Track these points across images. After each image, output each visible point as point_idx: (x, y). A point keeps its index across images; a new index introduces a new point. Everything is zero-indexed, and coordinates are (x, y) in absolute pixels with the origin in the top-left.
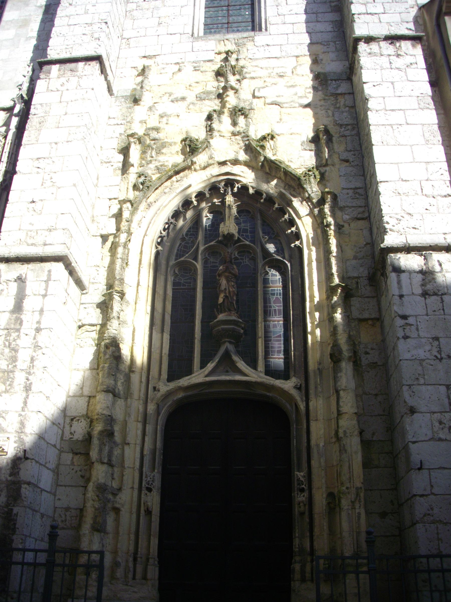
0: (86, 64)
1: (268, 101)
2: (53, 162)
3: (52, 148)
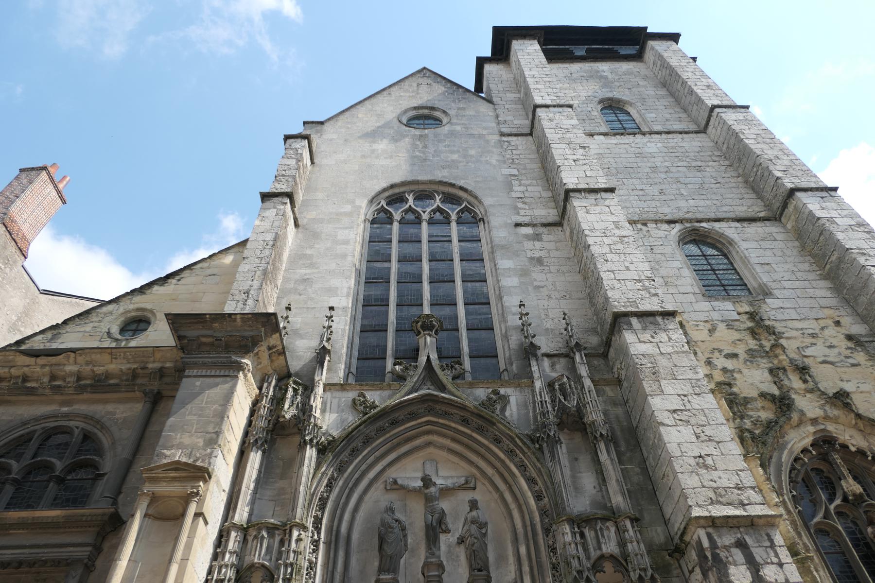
0: (664, 319)
1: (820, 360)
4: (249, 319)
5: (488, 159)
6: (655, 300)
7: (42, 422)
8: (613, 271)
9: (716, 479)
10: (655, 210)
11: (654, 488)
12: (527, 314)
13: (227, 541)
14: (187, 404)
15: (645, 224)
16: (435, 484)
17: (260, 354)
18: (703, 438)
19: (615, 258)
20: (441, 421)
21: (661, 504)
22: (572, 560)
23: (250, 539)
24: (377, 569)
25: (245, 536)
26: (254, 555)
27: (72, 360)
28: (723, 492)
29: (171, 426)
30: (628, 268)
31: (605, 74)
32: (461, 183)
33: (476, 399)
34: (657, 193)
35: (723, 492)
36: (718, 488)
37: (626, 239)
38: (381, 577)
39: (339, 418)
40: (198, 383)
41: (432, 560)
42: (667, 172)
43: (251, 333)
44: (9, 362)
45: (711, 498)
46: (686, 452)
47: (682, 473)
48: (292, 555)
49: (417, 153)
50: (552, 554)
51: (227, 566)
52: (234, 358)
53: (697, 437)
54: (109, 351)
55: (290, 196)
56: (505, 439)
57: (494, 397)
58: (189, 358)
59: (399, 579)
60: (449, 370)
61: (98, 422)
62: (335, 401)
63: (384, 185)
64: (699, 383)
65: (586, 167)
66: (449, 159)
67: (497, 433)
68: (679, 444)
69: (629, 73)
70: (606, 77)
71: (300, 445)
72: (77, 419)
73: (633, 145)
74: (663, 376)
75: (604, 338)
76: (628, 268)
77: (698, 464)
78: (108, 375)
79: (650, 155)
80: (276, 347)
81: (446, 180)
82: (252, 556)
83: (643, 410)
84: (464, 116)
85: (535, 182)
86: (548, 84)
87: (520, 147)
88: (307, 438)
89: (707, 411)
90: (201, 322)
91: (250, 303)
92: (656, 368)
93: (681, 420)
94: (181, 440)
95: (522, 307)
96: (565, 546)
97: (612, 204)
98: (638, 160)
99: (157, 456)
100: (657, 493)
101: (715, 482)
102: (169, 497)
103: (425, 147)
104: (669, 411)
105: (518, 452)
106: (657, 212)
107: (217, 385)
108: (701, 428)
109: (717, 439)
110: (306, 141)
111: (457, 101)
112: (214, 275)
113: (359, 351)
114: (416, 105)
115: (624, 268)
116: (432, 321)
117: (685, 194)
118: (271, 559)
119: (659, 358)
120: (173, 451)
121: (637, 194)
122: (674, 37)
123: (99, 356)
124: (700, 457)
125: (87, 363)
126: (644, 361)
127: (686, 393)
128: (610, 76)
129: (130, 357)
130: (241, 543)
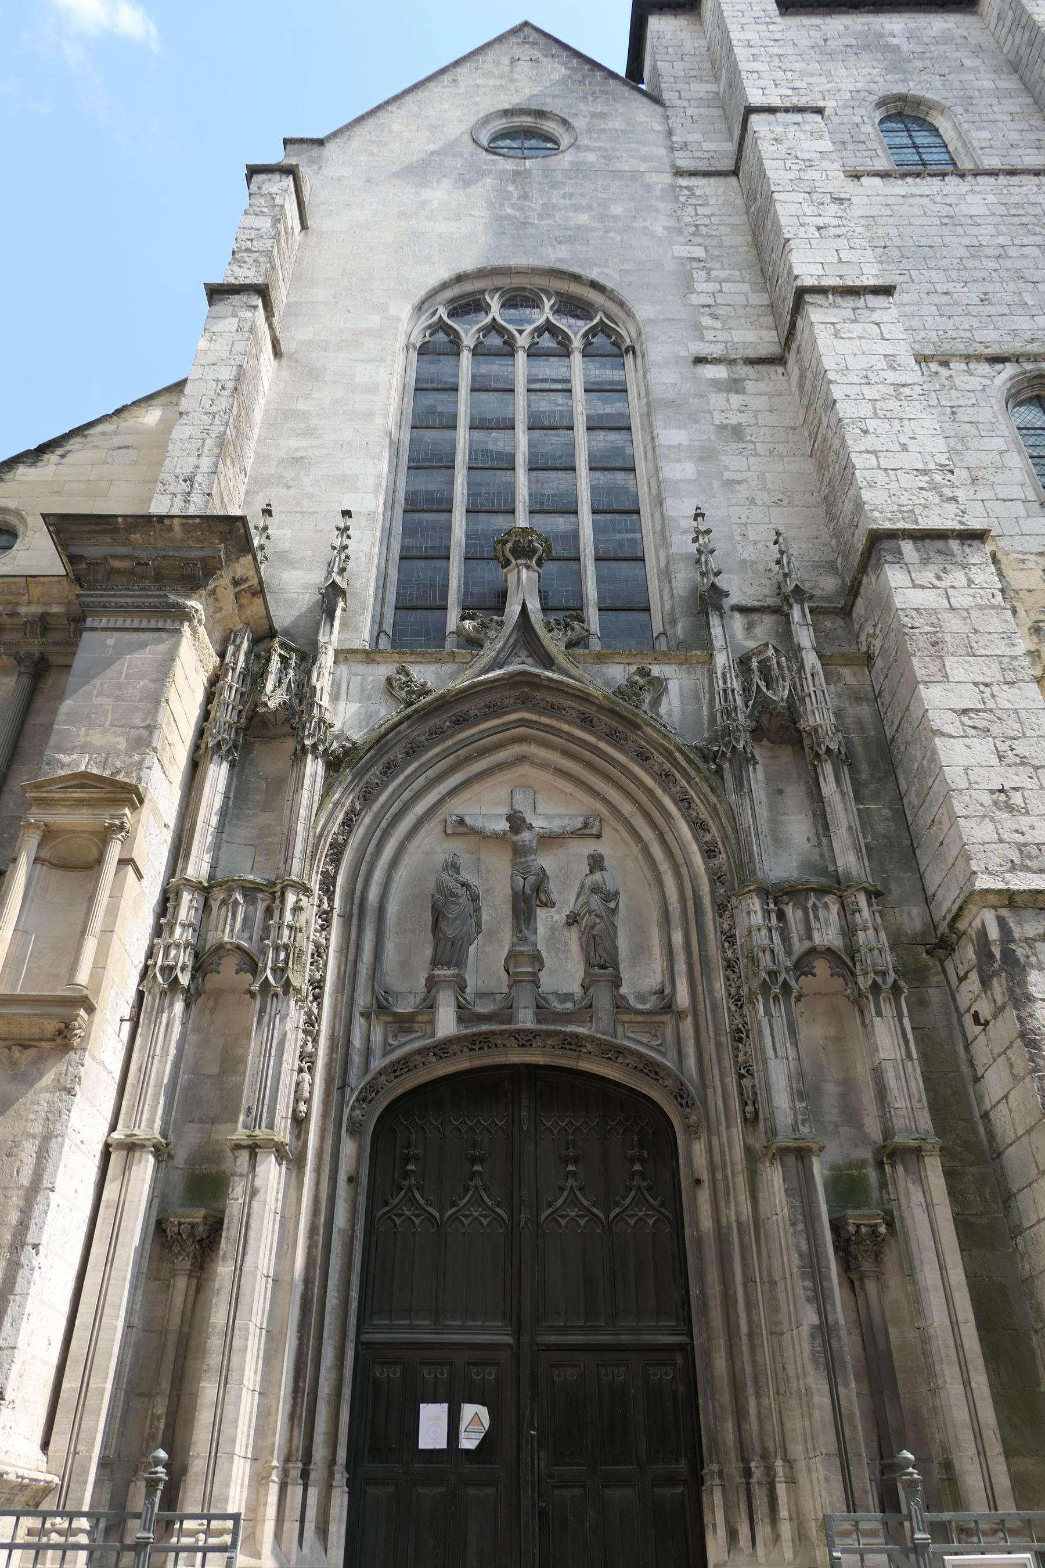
0: (963, 544)
2: (999, 719)
3: (983, 692)
4: (197, 527)
5: (648, 224)
6: (951, 508)
8: (875, 453)
9: (1024, 829)
10: (969, 334)
11: (912, 844)
12: (708, 532)
13: (177, 907)
14: (93, 677)
15: (945, 364)
16: (530, 827)
17: (218, 592)
18: (1011, 758)
19: (882, 426)
20: (544, 720)
21: (922, 870)
22: (761, 955)
23: (215, 905)
24: (429, 960)
25: (206, 900)
26: (223, 931)
28: (1035, 851)
29: (67, 714)
30: (904, 448)
31: (895, 41)
32: (594, 274)
33: (607, 684)
34: (977, 301)
35: (1035, 851)
36: (1026, 845)
37: (906, 391)
38: (437, 972)
39: (363, 710)
40: (111, 640)
41: (522, 949)
42: (999, 256)
43: (201, 554)
45: (1012, 861)
46: (976, 783)
47: (966, 817)
48: (286, 932)
49: (509, 211)
50: (726, 945)
51: (178, 946)
52: (173, 598)
53: (1001, 758)
55: (262, 291)
56: (656, 754)
57: (641, 681)
58: (91, 596)
59: (467, 977)
60: (560, 630)
62: (356, 681)
63: (445, 274)
64: (1015, 663)
65: (842, 243)
66: (572, 224)
67: (643, 743)
68: (966, 769)
69: (944, 39)
70: (896, 49)
71: (295, 754)
73: (938, 199)
74: (951, 650)
75: (848, 580)
76: (904, 448)
77: (995, 803)
79: (970, 221)
80: (246, 580)
81: (564, 267)
82: (219, 933)
83: (907, 708)
84: (604, 131)
85: (737, 273)
86: (776, 62)
87: (712, 201)
88: (307, 742)
89: (1023, 714)
90: (110, 531)
91: (197, 498)
92: (940, 635)
93: (974, 728)
94: (88, 739)
95: (700, 519)
96: (750, 932)
97: (886, 319)
98: (946, 230)
99: (48, 764)
100: (917, 851)
101: (1023, 834)
102: (74, 832)
103: (525, 196)
104: (954, 711)
105: (678, 776)
106: (972, 340)
107: (143, 645)
108: (1009, 743)
109: (1036, 763)
110: (291, 178)
111: (590, 98)
112: (127, 447)
113: (398, 594)
114: (507, 106)
115: (898, 448)
116: (531, 541)
117: (1031, 303)
118: (251, 938)
119: (946, 616)
120: (75, 756)
121: (936, 301)
124: (1001, 791)
126: (918, 621)
127: (988, 680)
128: (905, 47)
130: (200, 911)
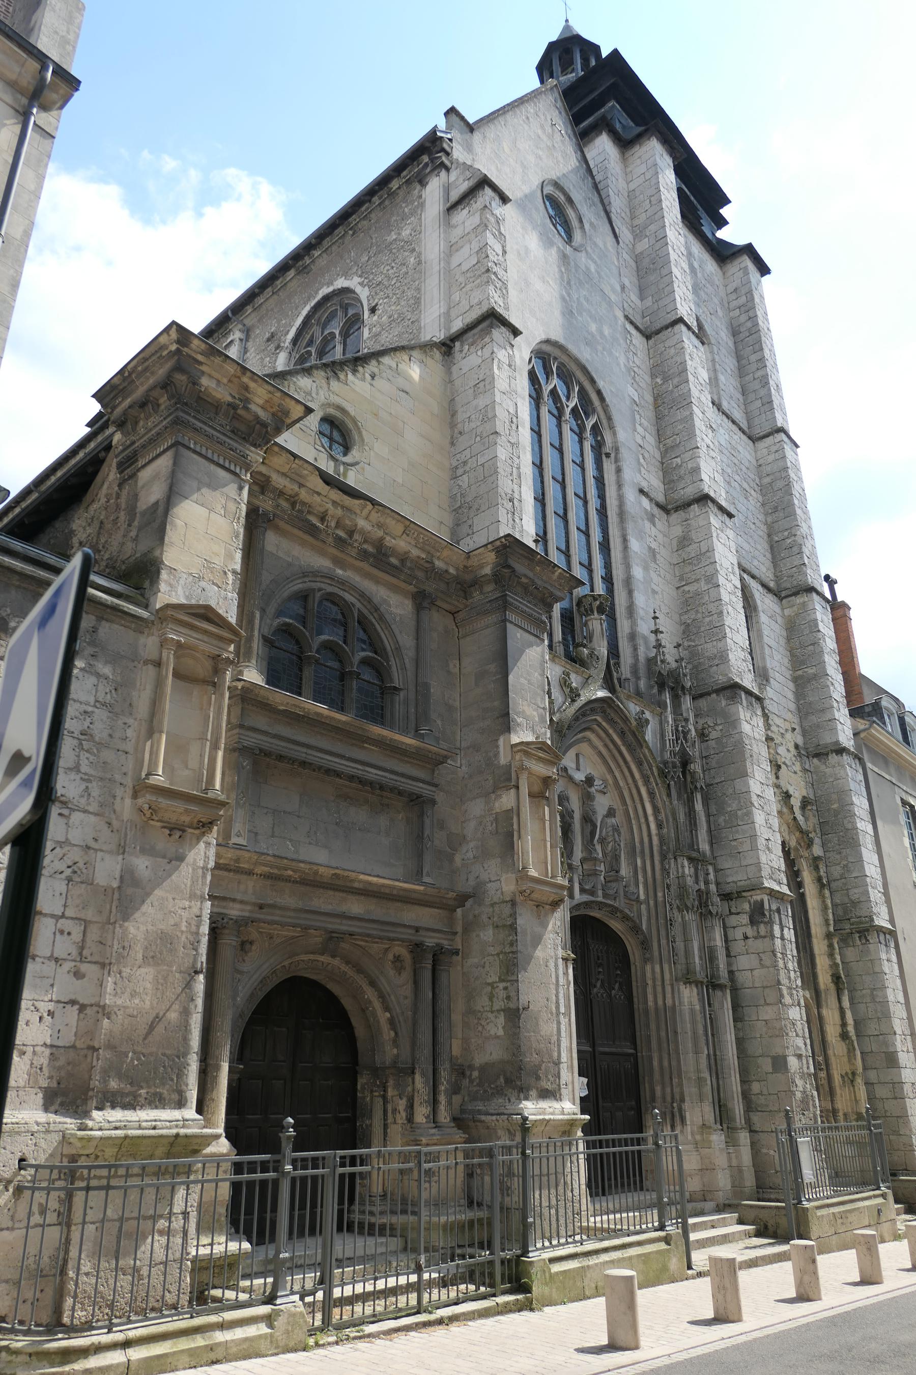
7: (318, 579)
20: (604, 724)
27: (365, 512)
32: (601, 384)
44: (301, 476)
54: (408, 523)
61: (377, 609)
72: (351, 592)
78: (393, 552)
81: (590, 369)
90: (530, 559)
110: (486, 187)
112: (407, 393)
122: (764, 270)
123: (394, 522)
125: (380, 526)
129: (421, 540)
